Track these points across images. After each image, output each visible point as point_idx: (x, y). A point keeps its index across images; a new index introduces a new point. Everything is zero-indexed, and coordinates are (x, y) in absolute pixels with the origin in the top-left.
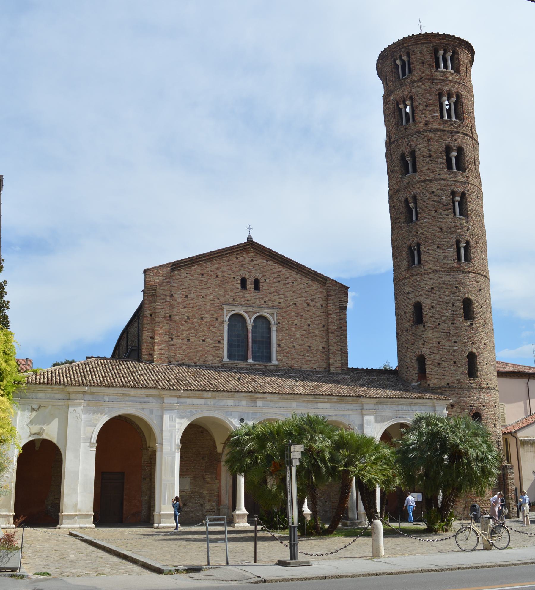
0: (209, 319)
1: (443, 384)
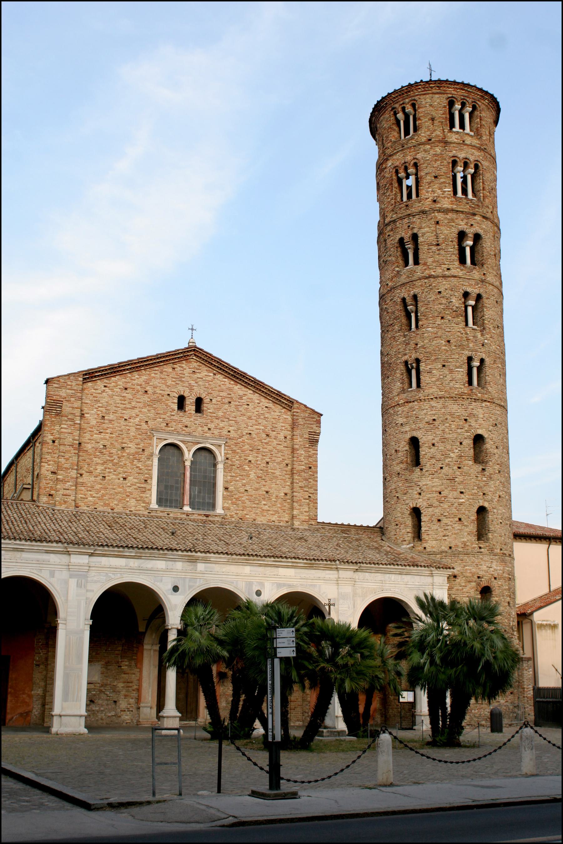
0: (133, 450)
1: (443, 548)
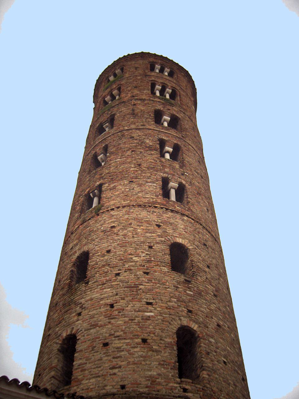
1: (108, 388)
